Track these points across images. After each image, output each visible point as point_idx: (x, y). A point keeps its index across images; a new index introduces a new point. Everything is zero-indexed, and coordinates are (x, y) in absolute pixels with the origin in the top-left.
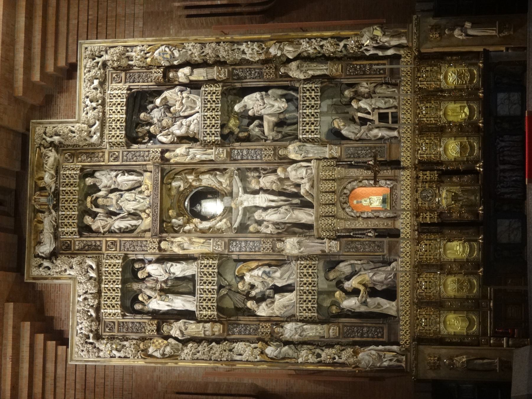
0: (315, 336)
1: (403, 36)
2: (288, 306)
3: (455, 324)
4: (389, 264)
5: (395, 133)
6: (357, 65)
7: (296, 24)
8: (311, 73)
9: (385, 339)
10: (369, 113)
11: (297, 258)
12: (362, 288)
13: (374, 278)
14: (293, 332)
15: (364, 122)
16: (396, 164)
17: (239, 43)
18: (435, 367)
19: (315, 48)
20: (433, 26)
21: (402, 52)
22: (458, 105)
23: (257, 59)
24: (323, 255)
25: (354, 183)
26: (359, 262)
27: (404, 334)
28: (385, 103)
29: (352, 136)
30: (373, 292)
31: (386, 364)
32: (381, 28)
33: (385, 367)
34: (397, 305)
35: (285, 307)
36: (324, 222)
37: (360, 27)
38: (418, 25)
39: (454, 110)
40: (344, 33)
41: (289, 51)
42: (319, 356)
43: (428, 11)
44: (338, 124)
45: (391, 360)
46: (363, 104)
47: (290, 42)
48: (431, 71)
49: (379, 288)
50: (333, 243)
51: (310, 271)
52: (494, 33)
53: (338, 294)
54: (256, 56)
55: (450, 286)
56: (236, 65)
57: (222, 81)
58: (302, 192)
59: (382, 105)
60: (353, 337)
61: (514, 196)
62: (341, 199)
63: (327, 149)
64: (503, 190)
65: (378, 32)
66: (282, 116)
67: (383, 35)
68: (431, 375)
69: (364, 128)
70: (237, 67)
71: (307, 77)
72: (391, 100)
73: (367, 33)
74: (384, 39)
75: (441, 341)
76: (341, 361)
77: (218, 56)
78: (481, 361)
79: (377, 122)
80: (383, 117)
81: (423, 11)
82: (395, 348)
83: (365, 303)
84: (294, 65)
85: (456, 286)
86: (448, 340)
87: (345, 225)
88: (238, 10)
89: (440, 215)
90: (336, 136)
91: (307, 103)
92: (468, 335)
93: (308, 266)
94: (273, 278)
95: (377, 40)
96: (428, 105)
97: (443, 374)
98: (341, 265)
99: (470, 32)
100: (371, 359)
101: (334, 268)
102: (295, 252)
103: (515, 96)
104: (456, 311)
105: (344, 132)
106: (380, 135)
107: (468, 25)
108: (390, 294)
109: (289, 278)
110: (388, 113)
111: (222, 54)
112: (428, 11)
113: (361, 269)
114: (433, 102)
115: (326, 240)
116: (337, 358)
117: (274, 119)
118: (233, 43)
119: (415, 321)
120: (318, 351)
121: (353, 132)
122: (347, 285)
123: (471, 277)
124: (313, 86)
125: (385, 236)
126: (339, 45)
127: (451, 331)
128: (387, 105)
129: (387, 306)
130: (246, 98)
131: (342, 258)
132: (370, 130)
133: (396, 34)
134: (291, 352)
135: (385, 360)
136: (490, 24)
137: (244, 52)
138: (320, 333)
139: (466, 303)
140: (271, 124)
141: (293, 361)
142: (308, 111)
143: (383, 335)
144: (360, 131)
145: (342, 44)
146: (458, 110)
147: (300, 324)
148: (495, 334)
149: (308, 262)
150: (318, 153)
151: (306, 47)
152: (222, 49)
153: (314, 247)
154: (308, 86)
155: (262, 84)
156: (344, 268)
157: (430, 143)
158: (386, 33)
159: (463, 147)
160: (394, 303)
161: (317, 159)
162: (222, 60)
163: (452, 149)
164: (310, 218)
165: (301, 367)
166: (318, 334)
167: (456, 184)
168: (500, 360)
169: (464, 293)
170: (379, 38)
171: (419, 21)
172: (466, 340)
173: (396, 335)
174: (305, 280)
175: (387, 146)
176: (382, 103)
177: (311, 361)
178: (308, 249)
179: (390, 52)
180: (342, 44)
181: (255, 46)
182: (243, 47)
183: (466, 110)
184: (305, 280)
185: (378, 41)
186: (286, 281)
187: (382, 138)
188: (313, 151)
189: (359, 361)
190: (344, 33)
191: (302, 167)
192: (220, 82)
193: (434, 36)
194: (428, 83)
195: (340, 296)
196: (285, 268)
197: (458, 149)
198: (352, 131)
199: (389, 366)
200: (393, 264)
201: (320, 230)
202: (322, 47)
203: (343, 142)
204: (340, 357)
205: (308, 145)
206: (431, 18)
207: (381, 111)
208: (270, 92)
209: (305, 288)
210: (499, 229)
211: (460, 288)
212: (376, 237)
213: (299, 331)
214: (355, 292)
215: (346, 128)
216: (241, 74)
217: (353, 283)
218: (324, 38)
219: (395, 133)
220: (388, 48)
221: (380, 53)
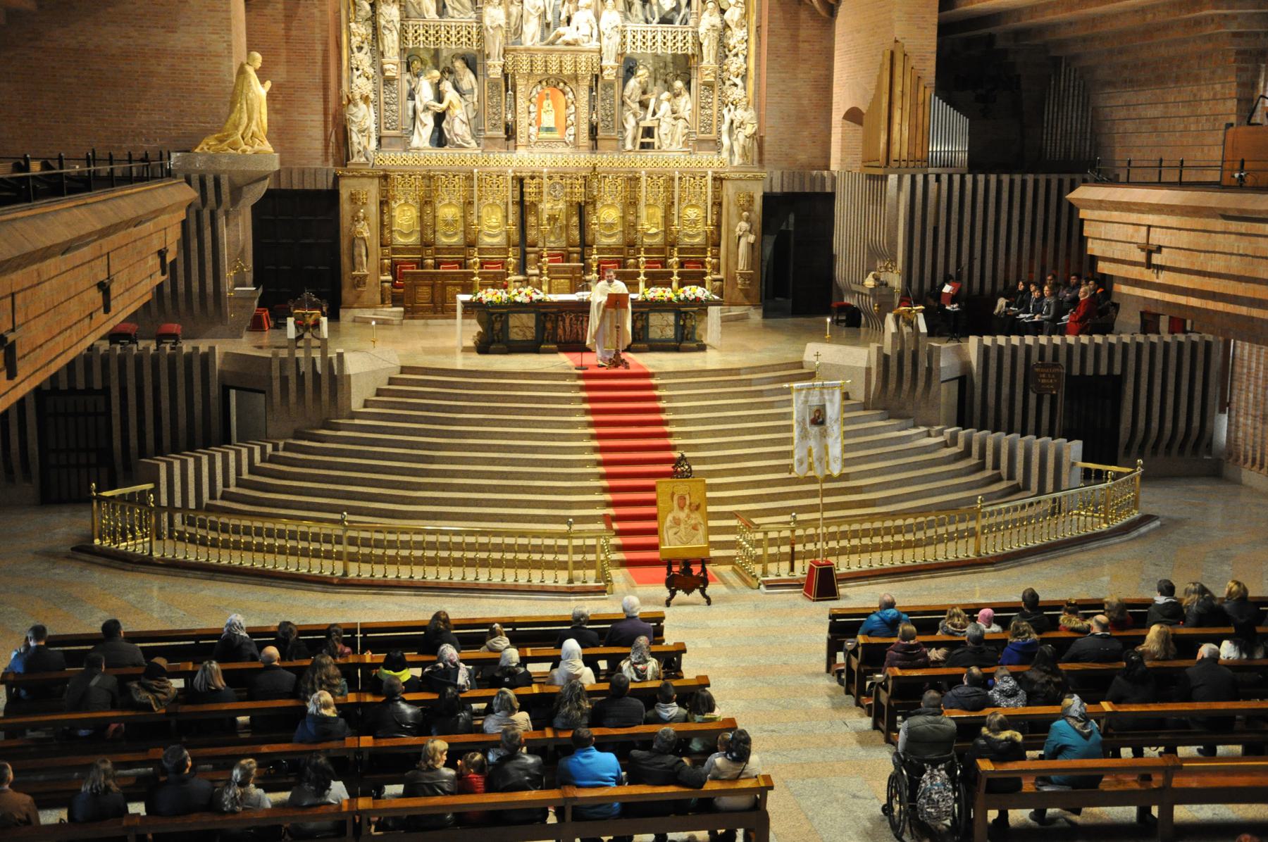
3: (405, 216)
4: (473, 136)
5: (629, 146)
7: (765, 23)
8: (705, 44)
10: (654, 113)
11: (480, 20)
12: (444, 106)
13: (457, 121)
15: (644, 105)
16: (594, 148)
18: (353, 199)
21: (725, 154)
22: (660, 220)
25: (571, 95)
27: (392, 158)
29: (627, 92)
30: (439, 118)
31: (355, 138)
34: (425, 148)
36: (524, 58)
37: (758, 108)
38: (756, 179)
39: (654, 215)
40: (751, 83)
41: (733, 15)
42: (360, 49)
44: (642, 73)
46: (665, 107)
47: (745, 15)
49: (444, 125)
51: (464, 40)
52: (741, 266)
53: (436, 73)
55: (448, 211)
58: (561, 30)
59: (662, 131)
61: (560, 332)
63: (612, 63)
64: (567, 321)
65: (750, 130)
68: (344, 194)
69: (636, 106)
71: (701, 37)
74: (741, 137)
75: (384, 203)
76: (355, 78)
78: (364, 253)
79: (642, 124)
80: (649, 132)
82: (374, 144)
83: (427, 108)
84: (716, 20)
85: (449, 218)
86: (386, 209)
89: (534, 204)
90: (629, 69)
91: (670, 37)
92: (392, 231)
97: (345, 207)
98: (472, 76)
99: (743, 241)
101: (468, 66)
102: (487, 21)
103: (670, 333)
104: (421, 217)
107: (752, 238)
108: (440, 139)
109: (454, 8)
119: (408, 174)
120: (366, 47)
122: (447, 86)
123: (461, 235)
124: (689, 45)
125: (507, 132)
127: (396, 213)
128: (663, 137)
129: (423, 135)
132: (635, 115)
134: (362, 13)
136: (751, 265)
139: (429, 232)
141: (352, 16)
142: (659, 37)
144: (633, 101)
145: (738, 81)
146: (655, 220)
147: (398, 26)
148: (394, 264)
151: (736, 37)
153: (495, 45)
154: (689, 38)
156: (468, 79)
159: (611, 226)
160: (427, 144)
161: (601, 50)
163: (608, 214)
164: (529, 38)
165: (344, 26)
167: (568, 218)
168: (366, 276)
169: (441, 227)
172: (386, 231)
173: (390, 145)
174: (453, 32)
179: (725, 139)
180: (738, 81)
183: (654, 230)
184: (453, 32)
188: (611, 46)
189: (356, 105)
190: (751, 83)
197: (609, 221)
200: (474, 144)
202: (736, 55)
203: (621, 81)
205: (617, 38)
209: (443, 33)
210: (524, 316)
211: (447, 223)
212: (507, 124)
214: (439, 98)
217: (450, 95)
219: (629, 146)
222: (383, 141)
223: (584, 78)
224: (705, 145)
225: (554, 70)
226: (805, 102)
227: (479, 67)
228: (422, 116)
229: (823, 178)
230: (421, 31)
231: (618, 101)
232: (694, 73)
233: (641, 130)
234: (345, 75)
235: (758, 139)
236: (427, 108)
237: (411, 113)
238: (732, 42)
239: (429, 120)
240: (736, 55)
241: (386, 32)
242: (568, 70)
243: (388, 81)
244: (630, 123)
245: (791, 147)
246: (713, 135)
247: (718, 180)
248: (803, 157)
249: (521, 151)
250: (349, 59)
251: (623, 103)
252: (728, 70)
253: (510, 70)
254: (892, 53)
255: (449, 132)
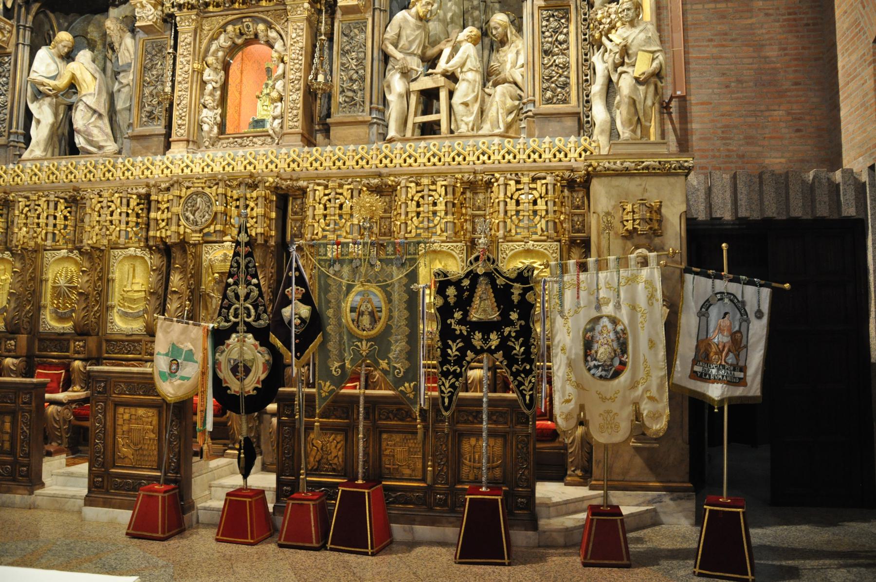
1: (634, 131)
5: (392, 133)
6: (567, 34)
20: (659, 211)
28: (466, 104)
32: (658, 75)
43: (710, 206)
48: (535, 212)
59: (457, 100)
65: (643, 65)
67: (637, 79)
72: (471, 119)
73: (642, 36)
81: (709, 191)
87: (183, 33)
95: (622, 64)
96: (441, 207)
105: (401, 15)
106: (389, 97)
110: (438, 112)
112: (710, 206)
113: (122, 83)
114: (450, 218)
121: (399, 35)
128: (459, 109)
132: (406, 74)
133: (641, 115)
157: (341, 216)
158: (642, 88)
170: (630, 70)
171: (677, 175)
176: (466, 95)
179: (599, 112)
185: (620, 69)
193: (629, 217)
194: (502, 204)
198: (403, 34)
206: (683, 208)
207: (443, 95)
215: (412, 20)
220: (609, 104)
221: (597, 88)
224: (554, 125)
226: (772, 52)
229: (835, 188)
235: (666, 97)
245: (750, 140)
246: (573, 104)
247: (578, 185)
248: (776, 161)
249: (178, 151)
251: (386, 58)
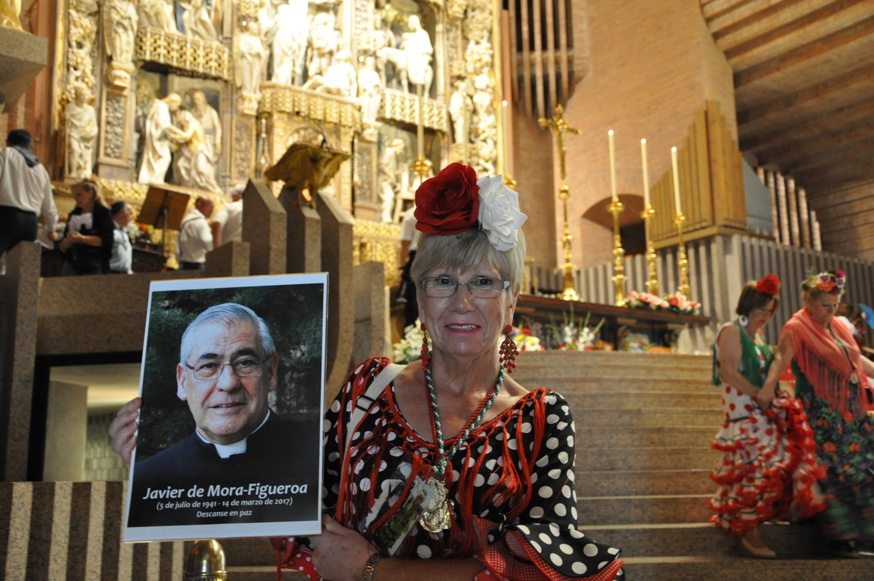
0: (113, 47)
2: (158, 20)
9: (103, 158)
12: (186, 135)
14: (122, 13)
17: (490, 39)
19: (484, 132)
23: (469, 59)
24: (233, 89)
26: (218, 141)
30: (175, 156)
31: (76, 145)
33: (70, 146)
35: (157, 14)
41: (483, 100)
42: (80, 46)
45: (81, 156)
49: (181, 163)
50: (255, 106)
54: (476, 57)
56: (463, 31)
57: (446, 10)
60: (107, 109)
62: (310, 131)
66: (403, 75)
70: (459, 32)
76: (72, 78)
77: (473, 10)
83: (164, 136)
84: (469, 101)
88: (514, 50)
93: (220, 62)
94: (197, 9)
98: (214, 113)
100: (83, 124)
111: (478, 15)
115: (258, 96)
116: (78, 73)
117: (400, 65)
118: (491, 32)
120: (88, 46)
126: (487, 161)
130: (425, 35)
131: (227, 116)
135: (82, 145)
137: (477, 43)
138: (121, 54)
140: (394, 59)
143: (107, 155)
145: (489, 166)
147: (135, 27)
149: (226, 63)
150: (369, 110)
151: (485, 122)
152: (486, 15)
155: (440, 59)
162: (470, 14)
166: (118, 51)
173: (110, 176)
175: (373, 205)
177: (73, 30)
178: (248, 67)
181: (487, 59)
182: (485, 44)
186: (192, 30)
187: (380, 200)
191: (351, 83)
192: (445, 5)
195: (173, 101)
196: (213, 30)
199: (71, 152)
201: (273, 90)
202: (485, 141)
204: (77, 78)
205: (379, 97)
208: (429, 68)
209: (189, 51)
213: (126, 23)
216: (452, 35)
218: (495, 143)
222: (102, 170)
223: (346, 133)
225: (319, 115)
227: (222, 104)
228: (157, 145)
230: (162, 42)
231: (375, 170)
232: (444, 153)
233: (400, 204)
234: (58, 73)
236: (164, 136)
237: (134, 147)
238: (482, 126)
239: (164, 150)
240: (485, 141)
241: (120, 30)
242: (333, 117)
243: (114, 93)
244: (388, 195)
250: (66, 56)
252: (477, 155)
253: (267, 107)
254: (706, 114)
255: (188, 171)
